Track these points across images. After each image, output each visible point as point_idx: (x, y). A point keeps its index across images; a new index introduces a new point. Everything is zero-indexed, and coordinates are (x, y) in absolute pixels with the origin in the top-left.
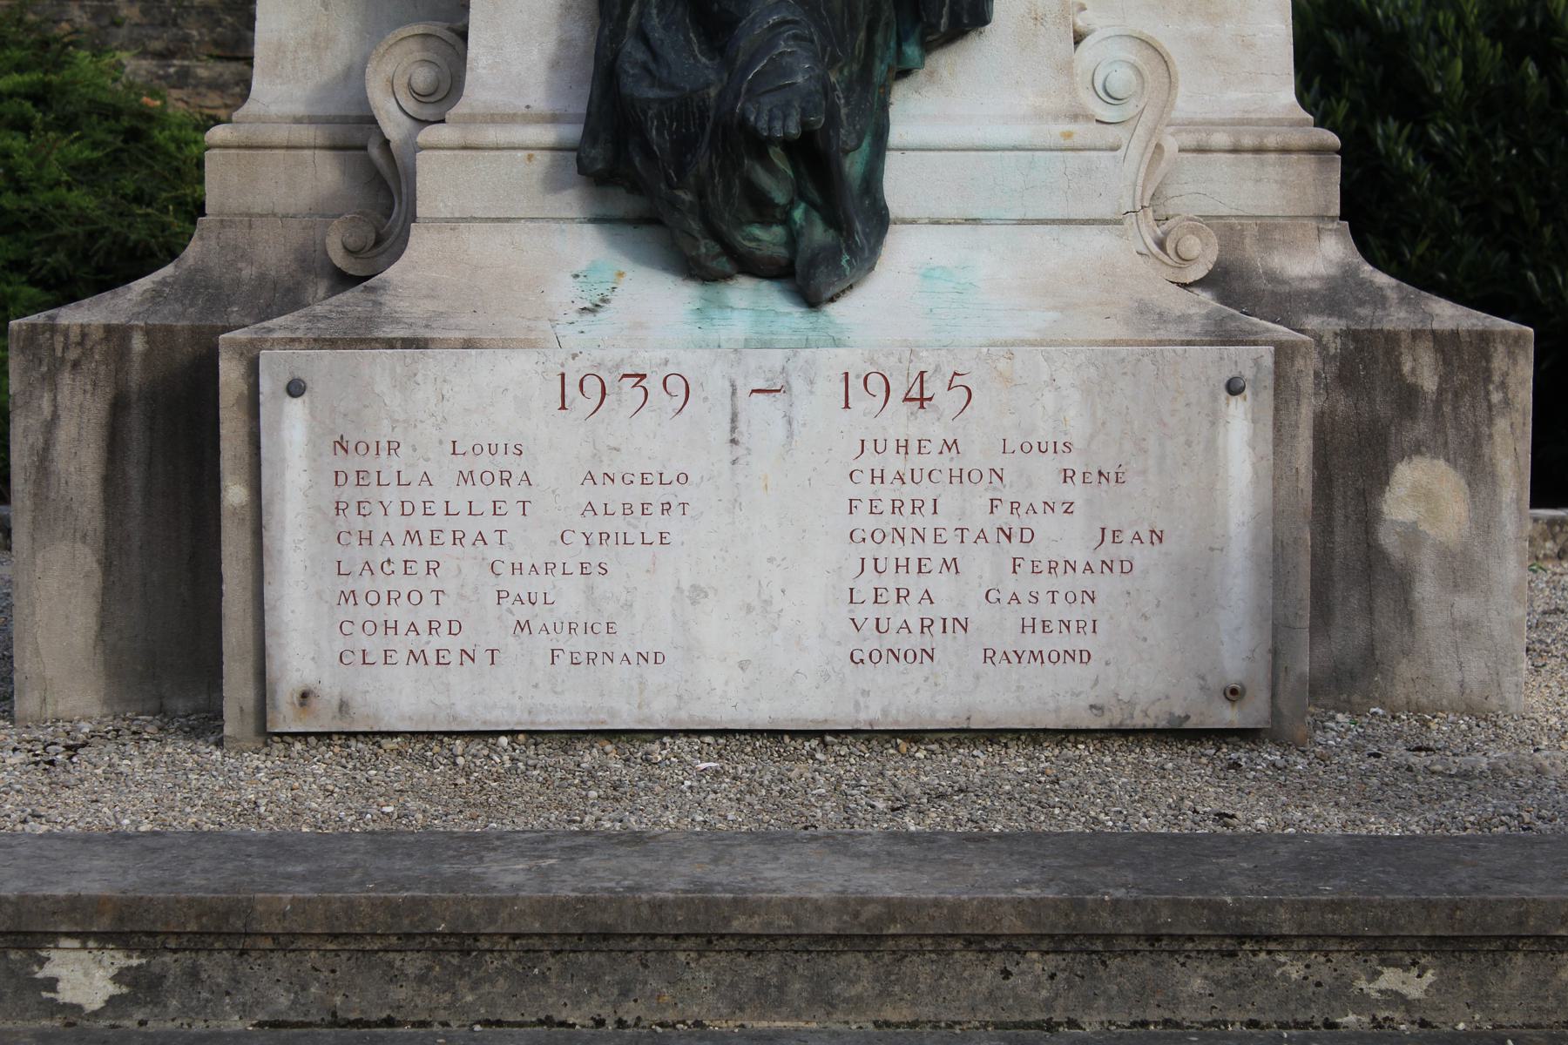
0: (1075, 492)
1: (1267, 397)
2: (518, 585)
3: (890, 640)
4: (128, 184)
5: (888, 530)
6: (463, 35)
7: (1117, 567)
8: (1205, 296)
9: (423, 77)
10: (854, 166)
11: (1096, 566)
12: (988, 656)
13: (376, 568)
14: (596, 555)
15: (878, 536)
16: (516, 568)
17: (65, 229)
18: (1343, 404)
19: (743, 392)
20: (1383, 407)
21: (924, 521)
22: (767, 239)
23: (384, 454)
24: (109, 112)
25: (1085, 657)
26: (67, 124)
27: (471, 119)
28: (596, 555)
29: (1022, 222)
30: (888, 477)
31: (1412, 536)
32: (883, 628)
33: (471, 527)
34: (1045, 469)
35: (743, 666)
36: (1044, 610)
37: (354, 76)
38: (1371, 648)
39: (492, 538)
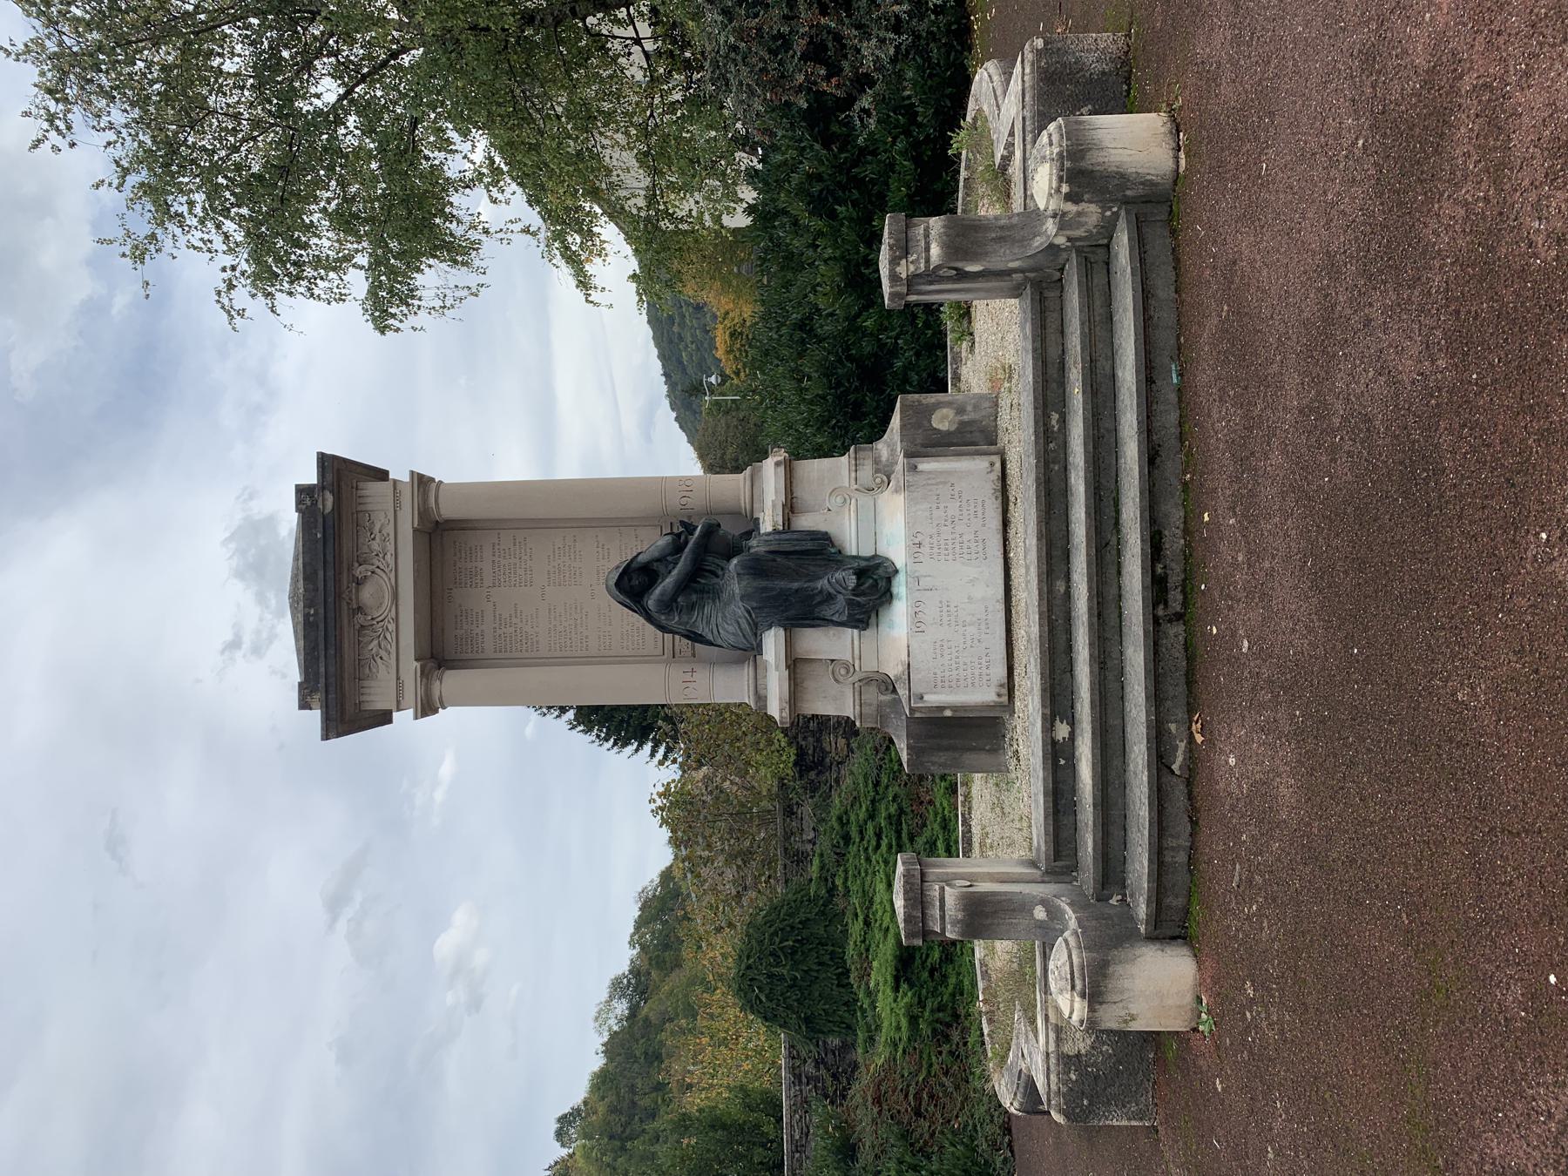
2: (969, 643)
3: (980, 550)
6: (833, 661)
10: (863, 564)
12: (984, 525)
14: (960, 623)
21: (950, 542)
22: (882, 584)
27: (853, 658)
28: (960, 623)
36: (972, 512)
38: (982, 431)
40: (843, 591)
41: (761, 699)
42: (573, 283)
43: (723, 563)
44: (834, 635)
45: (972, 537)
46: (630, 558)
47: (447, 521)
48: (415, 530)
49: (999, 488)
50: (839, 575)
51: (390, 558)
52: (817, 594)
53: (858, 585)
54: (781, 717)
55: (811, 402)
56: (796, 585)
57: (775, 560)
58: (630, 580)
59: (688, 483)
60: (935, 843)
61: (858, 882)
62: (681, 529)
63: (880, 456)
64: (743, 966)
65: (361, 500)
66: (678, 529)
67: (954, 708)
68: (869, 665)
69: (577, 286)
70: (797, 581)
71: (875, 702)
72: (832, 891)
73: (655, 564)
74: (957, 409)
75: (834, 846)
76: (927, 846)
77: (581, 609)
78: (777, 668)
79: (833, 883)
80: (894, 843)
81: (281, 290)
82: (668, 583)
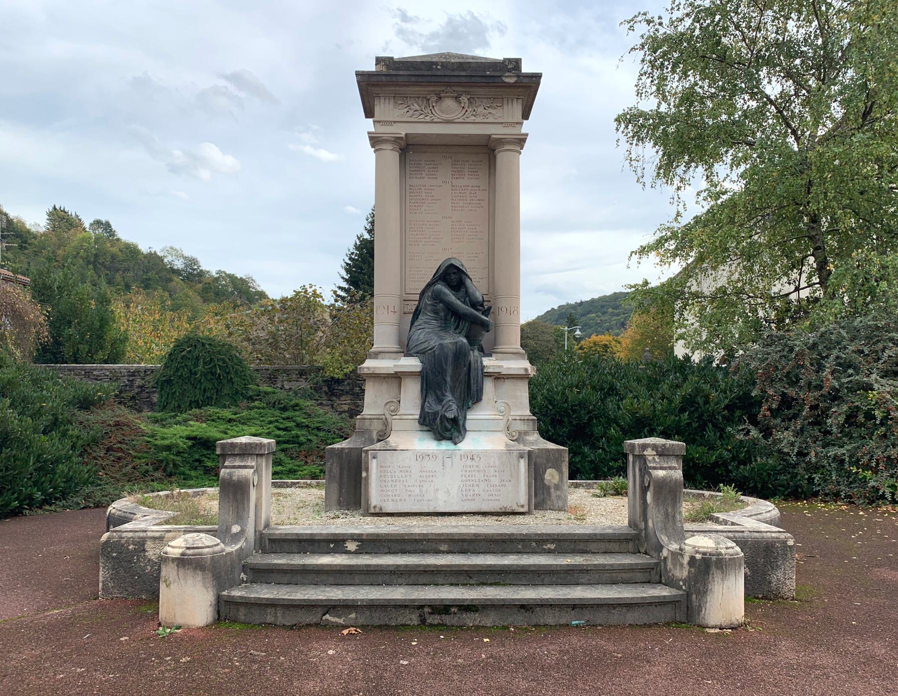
0: (497, 474)
2: (409, 489)
3: (468, 497)
6: (399, 402)
10: (461, 423)
14: (422, 484)
22: (448, 434)
25: (499, 500)
28: (422, 484)
33: (402, 479)
34: (492, 470)
36: (492, 493)
40: (444, 409)
41: (376, 355)
42: (644, 244)
43: (464, 333)
44: (416, 403)
45: (477, 493)
46: (468, 273)
47: (495, 157)
48: (489, 136)
49: (507, 511)
50: (454, 407)
52: (442, 392)
53: (447, 419)
54: (364, 368)
55: (563, 394)
56: (448, 379)
57: (465, 366)
58: (454, 273)
59: (515, 313)
60: (280, 465)
61: (256, 416)
62: (486, 307)
63: (529, 435)
64: (203, 341)
67: (367, 478)
68: (396, 425)
69: (641, 246)
70: (451, 380)
71: (372, 428)
72: (251, 399)
74: (558, 485)
75: (280, 401)
76: (279, 460)
77: (437, 242)
78: (395, 366)
79: (256, 400)
80: (281, 439)
81: (645, 55)
82: (451, 297)
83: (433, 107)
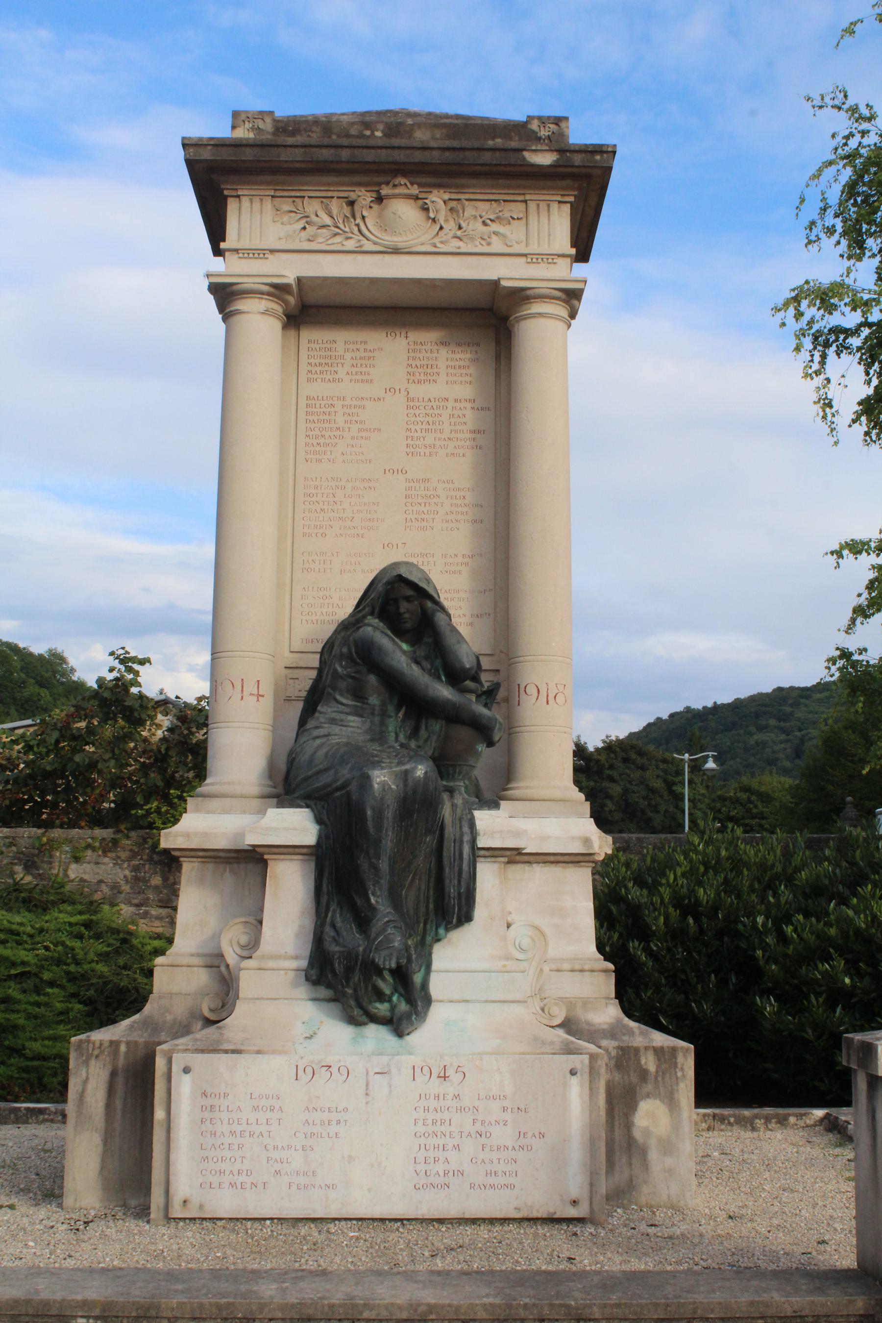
0: (508, 1116)
1: (586, 1076)
2: (275, 1155)
3: (431, 1180)
4: (121, 962)
5: (431, 1132)
6: (261, 922)
7: (525, 1148)
8: (561, 1032)
9: (244, 939)
10: (418, 978)
11: (517, 1148)
12: (472, 1186)
13: (217, 1146)
15: (426, 1135)
16: (275, 1148)
17: (95, 981)
18: (617, 1077)
19: (371, 1073)
20: (634, 1079)
21: (445, 1128)
22: (382, 1008)
23: (222, 1098)
24: (116, 931)
25: (512, 1186)
26: (98, 936)
27: (263, 958)
29: (486, 1002)
30: (431, 1110)
31: (647, 1132)
32: (428, 1174)
35: (369, 1190)
37: (216, 937)
38: (631, 1180)
39: (266, 1134)
45: (454, 1166)
48: (496, 283)
51: (454, 245)
52: (369, 900)
57: (429, 831)
58: (407, 599)
65: (543, 205)
66: (486, 679)
73: (430, 640)
83: (363, 218)
